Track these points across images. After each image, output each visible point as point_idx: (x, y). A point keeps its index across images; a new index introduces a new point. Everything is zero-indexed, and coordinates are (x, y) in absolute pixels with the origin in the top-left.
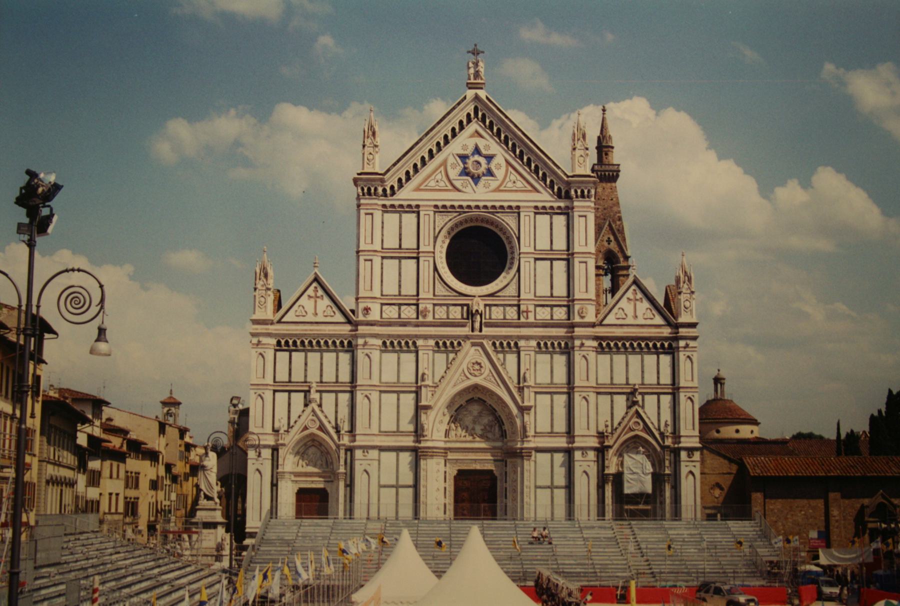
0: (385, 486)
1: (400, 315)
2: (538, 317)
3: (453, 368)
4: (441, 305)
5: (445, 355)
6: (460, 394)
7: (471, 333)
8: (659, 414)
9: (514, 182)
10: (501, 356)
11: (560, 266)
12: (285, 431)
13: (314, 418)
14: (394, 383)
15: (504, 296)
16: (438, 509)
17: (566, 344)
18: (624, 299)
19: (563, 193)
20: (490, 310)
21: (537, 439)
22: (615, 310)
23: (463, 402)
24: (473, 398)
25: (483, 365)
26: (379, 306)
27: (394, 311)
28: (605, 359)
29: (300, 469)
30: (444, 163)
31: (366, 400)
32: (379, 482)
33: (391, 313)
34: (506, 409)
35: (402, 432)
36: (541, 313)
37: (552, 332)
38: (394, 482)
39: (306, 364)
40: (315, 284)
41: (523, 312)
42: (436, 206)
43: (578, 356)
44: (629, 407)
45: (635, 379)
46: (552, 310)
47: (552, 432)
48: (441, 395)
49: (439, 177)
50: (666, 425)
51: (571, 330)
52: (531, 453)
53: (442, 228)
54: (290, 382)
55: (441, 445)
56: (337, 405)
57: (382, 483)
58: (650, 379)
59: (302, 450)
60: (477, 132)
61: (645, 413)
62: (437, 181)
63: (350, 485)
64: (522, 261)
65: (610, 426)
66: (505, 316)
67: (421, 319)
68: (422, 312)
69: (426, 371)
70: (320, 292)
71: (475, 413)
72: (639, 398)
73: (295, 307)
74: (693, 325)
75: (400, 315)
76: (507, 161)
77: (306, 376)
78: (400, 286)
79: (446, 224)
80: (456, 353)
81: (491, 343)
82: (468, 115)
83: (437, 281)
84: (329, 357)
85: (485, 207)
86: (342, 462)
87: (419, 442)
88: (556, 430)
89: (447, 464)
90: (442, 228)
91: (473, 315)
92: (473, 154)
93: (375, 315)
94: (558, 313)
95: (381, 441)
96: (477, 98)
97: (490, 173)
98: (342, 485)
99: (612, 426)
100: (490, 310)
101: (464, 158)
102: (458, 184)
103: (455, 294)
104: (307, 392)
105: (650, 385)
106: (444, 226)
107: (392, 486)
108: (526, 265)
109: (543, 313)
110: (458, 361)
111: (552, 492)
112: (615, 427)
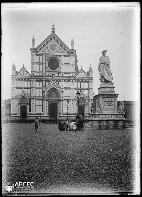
5: (48, 82)
6: (50, 89)
10: (58, 82)
16: (47, 110)
18: (80, 72)
22: (78, 75)
28: (76, 83)
31: (33, 90)
33: (38, 74)
42: (46, 55)
45: (82, 87)
48: (47, 89)
49: (46, 49)
58: (85, 87)
59: (22, 99)
60: (53, 41)
63: (30, 106)
67: (43, 75)
70: (24, 70)
72: (83, 90)
74: (92, 77)
76: (59, 47)
80: (50, 82)
82: (52, 38)
85: (55, 55)
93: (35, 75)
96: (53, 34)
98: (29, 106)
102: (50, 51)
104: (22, 89)
108: (63, 66)
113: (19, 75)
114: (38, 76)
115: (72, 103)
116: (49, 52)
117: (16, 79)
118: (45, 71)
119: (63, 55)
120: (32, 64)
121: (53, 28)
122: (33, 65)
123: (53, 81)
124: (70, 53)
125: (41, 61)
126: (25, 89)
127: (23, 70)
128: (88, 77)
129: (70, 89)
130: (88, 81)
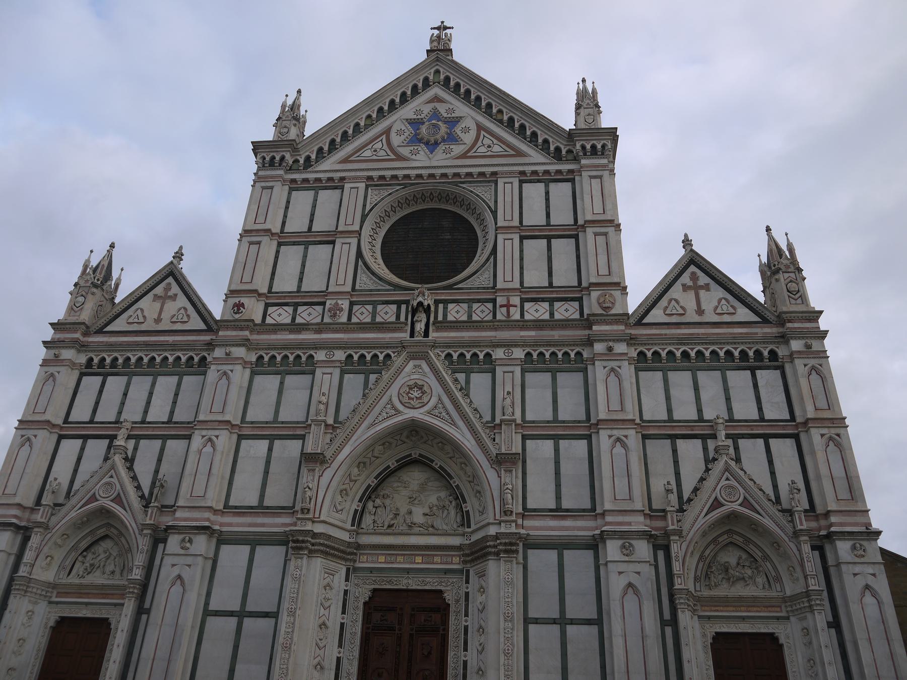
0: (217, 613)
1: (294, 319)
2: (527, 317)
3: (373, 394)
4: (363, 303)
5: (361, 377)
7: (408, 338)
8: (773, 473)
9: (489, 147)
10: (461, 377)
11: (563, 248)
12: (56, 505)
13: (115, 480)
14: (267, 423)
15: (470, 288)
16: (319, 667)
17: (579, 354)
18: (678, 286)
19: (564, 152)
20: (445, 308)
21: (527, 523)
22: (664, 302)
23: (393, 464)
24: (410, 455)
25: (425, 388)
26: (260, 307)
27: (285, 314)
28: (653, 380)
29: (73, 580)
30: (387, 132)
31: (208, 449)
32: (207, 604)
33: (281, 315)
34: (468, 469)
35: (268, 508)
36: (532, 311)
37: (553, 336)
38: (237, 607)
39: (125, 395)
40: (170, 280)
41: (501, 306)
42: (370, 178)
43: (599, 371)
44: (709, 461)
46: (551, 306)
47: (558, 509)
48: (347, 439)
50: (793, 488)
51: (587, 332)
52: (518, 545)
53: (376, 205)
54: (91, 421)
55: (345, 536)
56: (159, 460)
57: (213, 607)
58: (745, 409)
59: (84, 544)
61: (745, 473)
62: (375, 151)
63: (142, 611)
64: (500, 238)
65: (675, 490)
66: (470, 316)
67: (327, 320)
68: (329, 311)
69: (324, 399)
70: (175, 289)
71: (414, 485)
72: (729, 442)
73: (130, 312)
75: (294, 319)
77: (120, 413)
78: (301, 280)
79: (383, 199)
81: (443, 355)
82: (426, 79)
83: (359, 271)
84: (166, 384)
85: (444, 175)
86: (140, 560)
87: (295, 524)
88: (565, 505)
89: (352, 577)
90: (376, 205)
91: (414, 312)
92: (429, 120)
94: (562, 310)
95: (221, 525)
97: (452, 138)
98: (130, 606)
99: (680, 497)
100: (445, 308)
101: (415, 123)
102: (405, 151)
103: (388, 287)
104: (112, 438)
105: (746, 421)
106: (379, 202)
107: (231, 614)
109: (537, 311)
110: (382, 384)
111: (563, 634)
112: (685, 499)
113: (119, 325)
114: (277, 328)
115: (622, 582)
116: (400, 158)
117: (82, 359)
118: (348, 288)
119: (510, 174)
120: (245, 239)
121: (439, 37)
122: (254, 248)
123: (415, 366)
124: (569, 152)
125: (323, 224)
126: (138, 438)
127: (168, 288)
128: (765, 321)
129: (588, 438)
130: (773, 353)
